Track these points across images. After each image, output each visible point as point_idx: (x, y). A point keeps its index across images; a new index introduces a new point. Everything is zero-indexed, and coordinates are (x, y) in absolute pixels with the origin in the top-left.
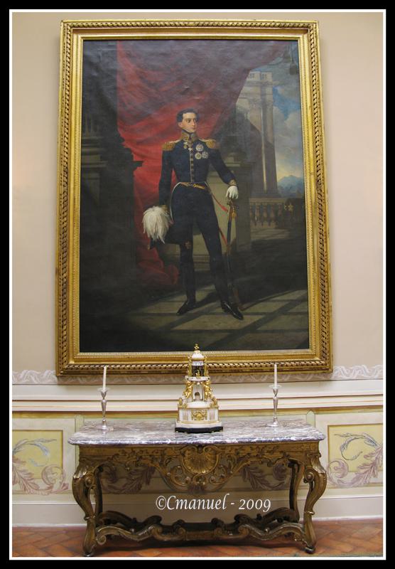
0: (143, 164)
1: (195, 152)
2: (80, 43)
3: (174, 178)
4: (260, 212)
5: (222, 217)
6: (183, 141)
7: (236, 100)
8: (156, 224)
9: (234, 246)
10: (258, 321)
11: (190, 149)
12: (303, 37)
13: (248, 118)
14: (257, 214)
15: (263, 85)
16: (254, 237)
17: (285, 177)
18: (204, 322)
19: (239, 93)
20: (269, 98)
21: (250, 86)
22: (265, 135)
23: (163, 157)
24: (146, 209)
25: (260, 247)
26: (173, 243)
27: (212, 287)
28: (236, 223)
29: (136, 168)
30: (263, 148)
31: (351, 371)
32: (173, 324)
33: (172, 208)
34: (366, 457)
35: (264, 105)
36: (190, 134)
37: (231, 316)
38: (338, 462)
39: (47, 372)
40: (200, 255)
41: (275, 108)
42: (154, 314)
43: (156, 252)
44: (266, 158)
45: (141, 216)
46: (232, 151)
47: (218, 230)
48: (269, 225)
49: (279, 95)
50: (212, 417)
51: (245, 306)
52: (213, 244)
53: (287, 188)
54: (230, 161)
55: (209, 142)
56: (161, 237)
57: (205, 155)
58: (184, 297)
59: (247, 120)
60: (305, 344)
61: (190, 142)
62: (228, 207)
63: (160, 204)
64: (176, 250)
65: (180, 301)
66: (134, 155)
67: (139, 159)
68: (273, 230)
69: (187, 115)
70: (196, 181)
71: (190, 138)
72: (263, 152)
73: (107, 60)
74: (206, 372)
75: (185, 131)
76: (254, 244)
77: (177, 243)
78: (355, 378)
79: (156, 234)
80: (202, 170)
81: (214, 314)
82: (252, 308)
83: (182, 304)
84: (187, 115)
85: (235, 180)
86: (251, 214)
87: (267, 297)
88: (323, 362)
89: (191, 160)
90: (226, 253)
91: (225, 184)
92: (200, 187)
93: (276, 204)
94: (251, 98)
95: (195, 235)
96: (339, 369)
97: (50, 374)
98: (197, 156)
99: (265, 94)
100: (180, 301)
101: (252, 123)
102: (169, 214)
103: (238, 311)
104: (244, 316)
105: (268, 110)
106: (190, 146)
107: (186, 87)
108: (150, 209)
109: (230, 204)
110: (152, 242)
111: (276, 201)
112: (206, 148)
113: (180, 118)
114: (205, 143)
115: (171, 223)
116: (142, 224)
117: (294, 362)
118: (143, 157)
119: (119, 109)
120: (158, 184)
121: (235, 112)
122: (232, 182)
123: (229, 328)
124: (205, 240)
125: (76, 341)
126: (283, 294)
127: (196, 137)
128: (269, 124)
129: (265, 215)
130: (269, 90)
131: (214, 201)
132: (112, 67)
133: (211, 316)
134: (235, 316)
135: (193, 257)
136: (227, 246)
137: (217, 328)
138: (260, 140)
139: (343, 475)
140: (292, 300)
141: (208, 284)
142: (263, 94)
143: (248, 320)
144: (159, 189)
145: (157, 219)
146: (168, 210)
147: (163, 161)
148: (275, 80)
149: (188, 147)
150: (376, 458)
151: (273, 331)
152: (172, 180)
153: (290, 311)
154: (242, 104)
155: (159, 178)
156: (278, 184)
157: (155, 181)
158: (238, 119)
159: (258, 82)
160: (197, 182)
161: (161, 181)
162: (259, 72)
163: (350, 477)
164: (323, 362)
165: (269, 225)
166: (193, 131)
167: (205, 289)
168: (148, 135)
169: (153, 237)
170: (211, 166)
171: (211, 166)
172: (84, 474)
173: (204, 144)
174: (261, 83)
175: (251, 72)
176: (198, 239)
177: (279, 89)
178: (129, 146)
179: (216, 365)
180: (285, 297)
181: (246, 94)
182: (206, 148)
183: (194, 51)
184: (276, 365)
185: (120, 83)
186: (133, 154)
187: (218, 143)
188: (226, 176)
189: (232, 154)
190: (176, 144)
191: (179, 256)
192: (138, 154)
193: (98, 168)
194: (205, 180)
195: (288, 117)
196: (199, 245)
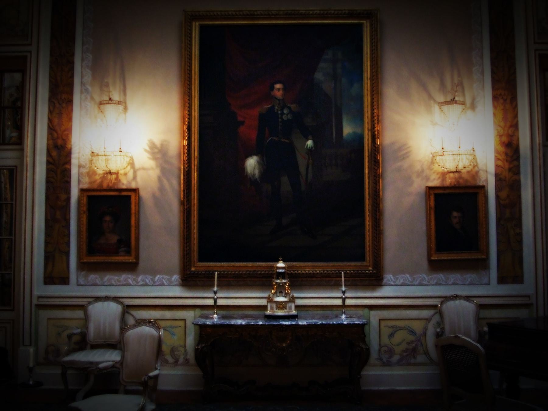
2: (197, 29)
5: (302, 162)
6: (273, 107)
8: (254, 169)
11: (279, 112)
12: (367, 22)
31: (397, 279)
34: (408, 343)
36: (279, 100)
38: (387, 346)
39: (174, 277)
50: (290, 308)
55: (293, 106)
56: (258, 180)
57: (290, 117)
60: (362, 258)
63: (256, 155)
71: (279, 104)
74: (287, 276)
75: (276, 98)
78: (399, 284)
84: (278, 86)
88: (374, 271)
92: (286, 141)
96: (388, 277)
97: (176, 278)
98: (285, 117)
108: (250, 158)
112: (291, 111)
113: (272, 88)
117: (354, 271)
125: (195, 255)
131: (296, 151)
139: (391, 357)
149: (278, 111)
150: (416, 345)
154: (319, 76)
163: (396, 358)
164: (374, 271)
172: (204, 345)
173: (289, 108)
176: (285, 179)
179: (296, 272)
184: (343, 273)
190: (269, 108)
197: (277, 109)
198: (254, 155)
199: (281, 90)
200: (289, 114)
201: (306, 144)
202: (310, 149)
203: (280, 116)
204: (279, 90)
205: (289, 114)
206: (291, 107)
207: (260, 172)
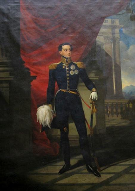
0: (37, 78)
1: (70, 70)
3: (56, 87)
4: (111, 109)
5: (87, 111)
6: (62, 63)
7: (96, 37)
8: (45, 116)
9: (94, 130)
10: (110, 178)
11: (67, 68)
13: (104, 48)
14: (109, 110)
15: (113, 27)
16: (108, 125)
17: (127, 86)
18: (77, 179)
19: (98, 33)
20: (117, 35)
21: (105, 28)
22: (115, 59)
23: (49, 74)
25: (112, 131)
26: (56, 128)
27: (81, 156)
28: (96, 116)
29: (32, 80)
30: (113, 67)
32: (56, 180)
33: (55, 105)
35: (114, 40)
36: (67, 58)
37: (93, 175)
40: (73, 136)
41: (121, 42)
42: (44, 174)
43: (45, 134)
44: (115, 74)
45: (36, 111)
46: (94, 70)
47: (84, 120)
48: (117, 116)
49: (123, 34)
51: (102, 168)
52: (82, 129)
53: (128, 93)
54: (92, 76)
55: (79, 64)
57: (76, 72)
58: (63, 163)
59: (103, 50)
61: (67, 64)
62: (91, 106)
63: (47, 103)
64: (58, 132)
65: (60, 165)
66: (31, 72)
67: (35, 75)
68: (120, 120)
69: (65, 47)
70: (70, 89)
71: (67, 62)
72: (113, 70)
73: (14, 12)
76: (107, 128)
77: (58, 128)
79: (45, 122)
80: (74, 81)
81: (82, 173)
82: (106, 169)
83: (62, 167)
84: (65, 47)
85: (96, 89)
86: (105, 110)
87: (116, 163)
89: (68, 75)
90: (89, 135)
91: (89, 91)
92: (73, 93)
93: (121, 103)
94: (106, 36)
95: (70, 123)
98: (72, 73)
99: (115, 33)
100: (60, 165)
102: (53, 110)
103: (97, 171)
104: (102, 175)
105: (117, 43)
106: (66, 66)
107: (64, 29)
108: (41, 107)
109: (92, 103)
110: (42, 128)
111: (122, 102)
112: (77, 68)
113: (60, 48)
114: (76, 64)
115: (55, 115)
116: (36, 116)
118: (37, 73)
119: (22, 43)
120: (46, 90)
121: (95, 45)
122: (94, 89)
123: (91, 182)
124: (76, 126)
126: (126, 161)
127: (71, 60)
128: (117, 52)
129: (115, 110)
130: (117, 31)
131: (82, 101)
132: (17, 16)
133: (80, 175)
134: (95, 175)
135: (69, 137)
136: (91, 130)
137: (84, 182)
138: (111, 63)
140: (132, 165)
141: (78, 154)
142: (113, 33)
143: (104, 177)
144: (47, 94)
145: (46, 113)
146: (53, 107)
147: (50, 75)
148: (121, 25)
151: (120, 184)
152: (56, 88)
153: (131, 171)
154: (100, 39)
155: (47, 87)
157: (44, 89)
158: (97, 49)
159: (110, 26)
160: (71, 89)
161: (48, 89)
162: (111, 19)
165: (117, 116)
168: (40, 59)
169: (43, 124)
170: (80, 79)
171: (80, 79)
173: (76, 65)
174: (112, 26)
175: (105, 19)
176: (72, 126)
177: (123, 30)
178: (28, 66)
180: (127, 163)
181: (103, 33)
182: (77, 68)
183: (69, 6)
185: (22, 26)
186: (30, 71)
187: (85, 65)
188: (90, 85)
189: (94, 71)
190: (58, 65)
191: (60, 137)
192: (34, 72)
193: (8, 80)
194: (77, 88)
195: (129, 48)
196: (73, 130)
197: (65, 66)
198: (45, 104)
199: (68, 50)
200: (75, 70)
201: (91, 95)
202: (94, 99)
203: (67, 72)
204: (66, 50)
205: (75, 70)
207: (51, 119)
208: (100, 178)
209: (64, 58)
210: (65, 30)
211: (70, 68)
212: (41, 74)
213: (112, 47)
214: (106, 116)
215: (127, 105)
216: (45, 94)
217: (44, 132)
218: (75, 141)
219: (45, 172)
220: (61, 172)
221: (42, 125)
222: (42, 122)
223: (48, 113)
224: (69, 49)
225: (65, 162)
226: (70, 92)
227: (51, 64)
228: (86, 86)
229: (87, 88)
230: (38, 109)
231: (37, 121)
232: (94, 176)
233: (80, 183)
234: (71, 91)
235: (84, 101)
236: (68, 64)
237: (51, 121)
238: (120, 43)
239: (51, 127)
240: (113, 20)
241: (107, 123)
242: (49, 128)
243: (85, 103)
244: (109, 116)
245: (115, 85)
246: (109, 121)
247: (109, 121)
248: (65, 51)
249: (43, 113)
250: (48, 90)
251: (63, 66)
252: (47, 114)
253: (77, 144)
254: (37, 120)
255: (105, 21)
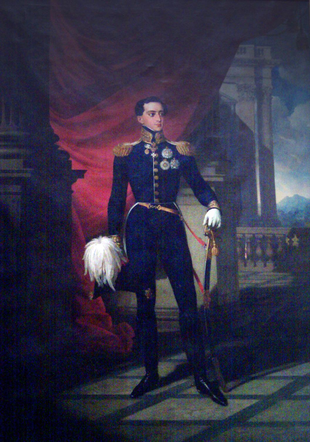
0: (86, 174)
1: (160, 159)
6: (143, 144)
11: (154, 155)
13: (237, 112)
16: (244, 284)
17: (287, 198)
23: (114, 166)
24: (88, 240)
26: (127, 290)
27: (183, 356)
28: (218, 260)
30: (257, 155)
32: (126, 412)
33: (126, 236)
36: (154, 133)
37: (209, 400)
45: (82, 251)
46: (213, 160)
47: (190, 272)
48: (265, 266)
51: (230, 384)
57: (174, 164)
58: (142, 371)
59: (235, 114)
61: (154, 144)
62: (207, 240)
63: (108, 233)
68: (272, 273)
70: (161, 202)
71: (153, 140)
72: (257, 161)
76: (241, 291)
81: (184, 396)
83: (139, 381)
84: (150, 106)
85: (217, 201)
87: (262, 373)
89: (155, 170)
90: (202, 306)
92: (167, 210)
93: (274, 238)
94: (241, 83)
95: (159, 279)
98: (164, 166)
99: (261, 78)
101: (242, 119)
102: (122, 248)
104: (229, 401)
106: (153, 150)
107: (149, 65)
108: (95, 241)
109: (209, 235)
110: (95, 290)
112: (176, 155)
113: (140, 110)
115: (126, 261)
116: (83, 262)
118: (85, 164)
120: (106, 203)
122: (213, 203)
123: (205, 417)
129: (259, 251)
131: (187, 230)
133: (181, 400)
134: (214, 400)
135: (156, 310)
136: (205, 295)
137: (187, 417)
141: (176, 352)
145: (105, 255)
146: (121, 242)
147: (115, 171)
149: (151, 152)
151: (272, 424)
153: (298, 393)
155: (109, 195)
156: (278, 208)
162: (253, 46)
165: (265, 266)
166: (158, 129)
167: (173, 358)
169: (98, 281)
170: (182, 179)
171: (182, 179)
173: (173, 148)
175: (240, 46)
177: (281, 70)
180: (288, 372)
182: (176, 155)
186: (71, 159)
187: (194, 148)
189: (213, 163)
190: (134, 147)
192: (79, 161)
194: (175, 200)
195: (293, 111)
197: (149, 150)
199: (157, 113)
200: (172, 158)
202: (213, 225)
204: (153, 113)
205: (172, 158)
206: (176, 146)
207: (115, 269)
208: (225, 408)
209: (148, 133)
210: (149, 68)
211: (162, 155)
212: (96, 166)
213: (256, 108)
214: (241, 264)
215: (288, 240)
216: (104, 212)
217: (100, 298)
218: (169, 320)
219: (99, 392)
220: (138, 392)
221: (96, 283)
222: (95, 275)
223: (111, 256)
224: (160, 111)
225: (147, 370)
226: (160, 209)
227: (119, 145)
228: (196, 195)
229: (198, 203)
230: (86, 246)
231: (85, 274)
232: (212, 402)
233: (179, 419)
234: (162, 205)
235: (188, 228)
236: (157, 145)
237: (116, 274)
238: (273, 99)
239: (115, 288)
240: (258, 47)
241: (240, 281)
242: (112, 289)
243: (193, 233)
244: (248, 264)
245: (261, 194)
246: (246, 277)
247: (246, 277)
248: (149, 115)
249: (99, 255)
250: (111, 203)
251: (146, 149)
252: (108, 257)
253: (175, 326)
254: (84, 271)
255: (239, 51)
